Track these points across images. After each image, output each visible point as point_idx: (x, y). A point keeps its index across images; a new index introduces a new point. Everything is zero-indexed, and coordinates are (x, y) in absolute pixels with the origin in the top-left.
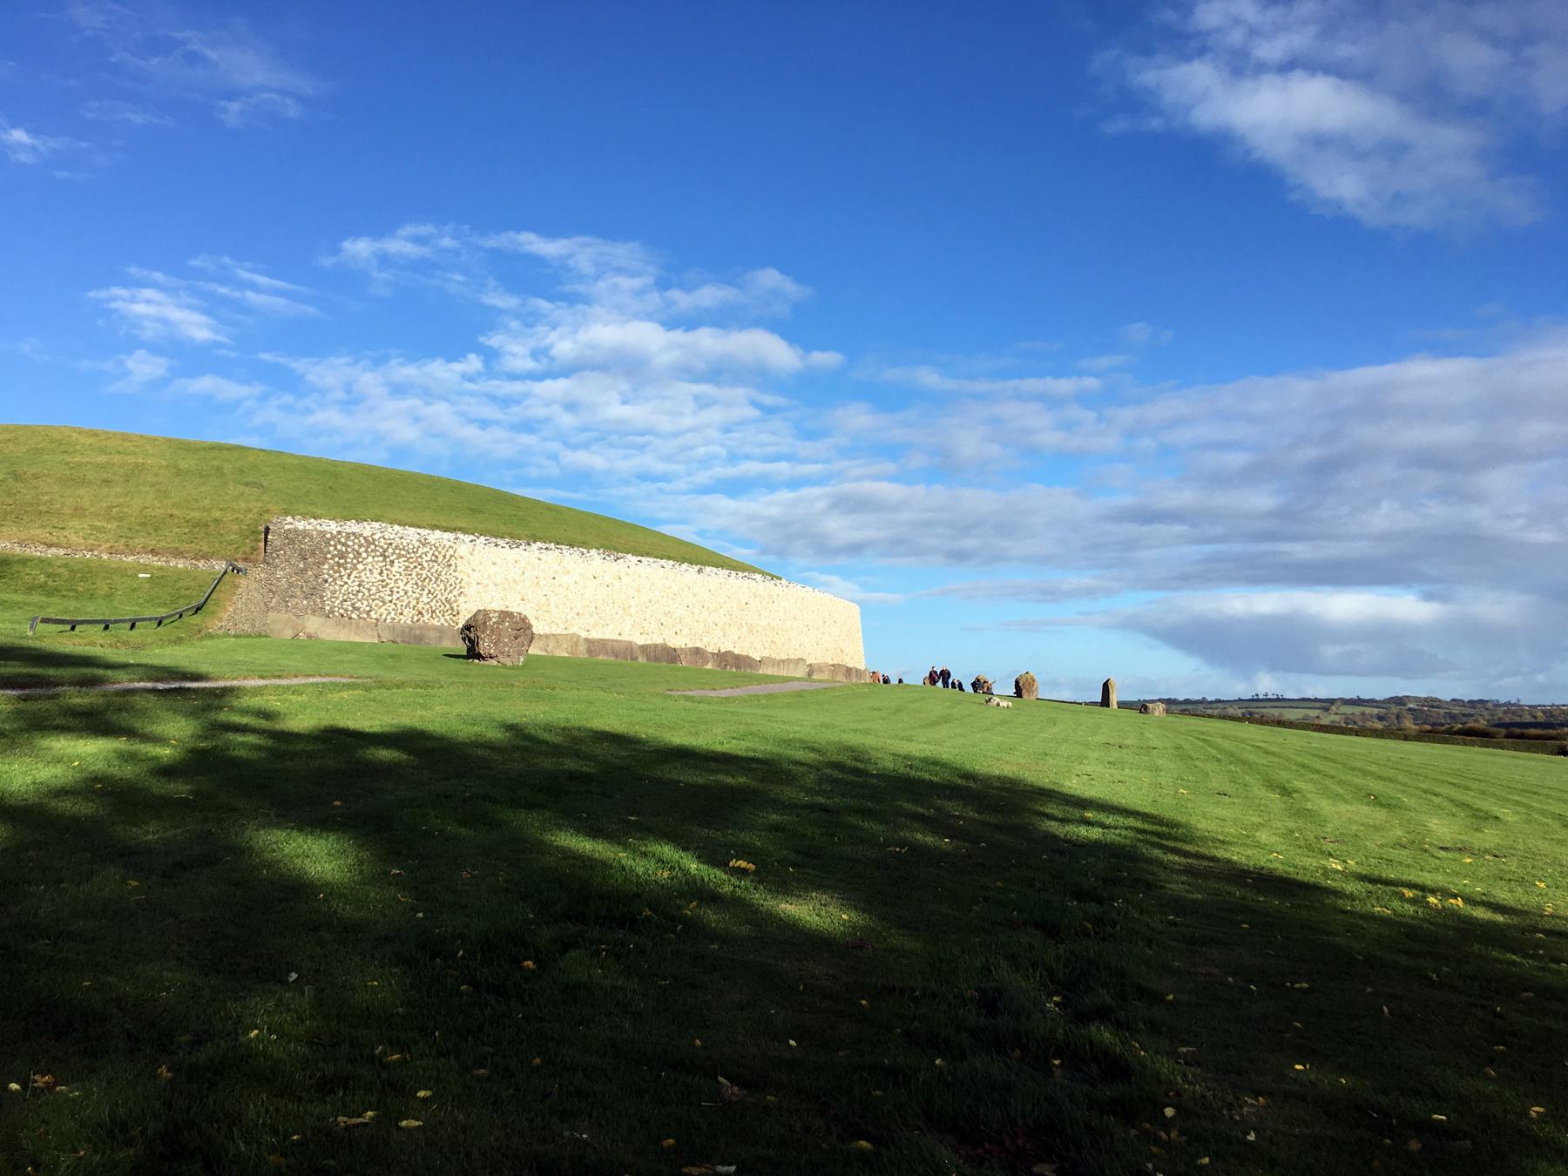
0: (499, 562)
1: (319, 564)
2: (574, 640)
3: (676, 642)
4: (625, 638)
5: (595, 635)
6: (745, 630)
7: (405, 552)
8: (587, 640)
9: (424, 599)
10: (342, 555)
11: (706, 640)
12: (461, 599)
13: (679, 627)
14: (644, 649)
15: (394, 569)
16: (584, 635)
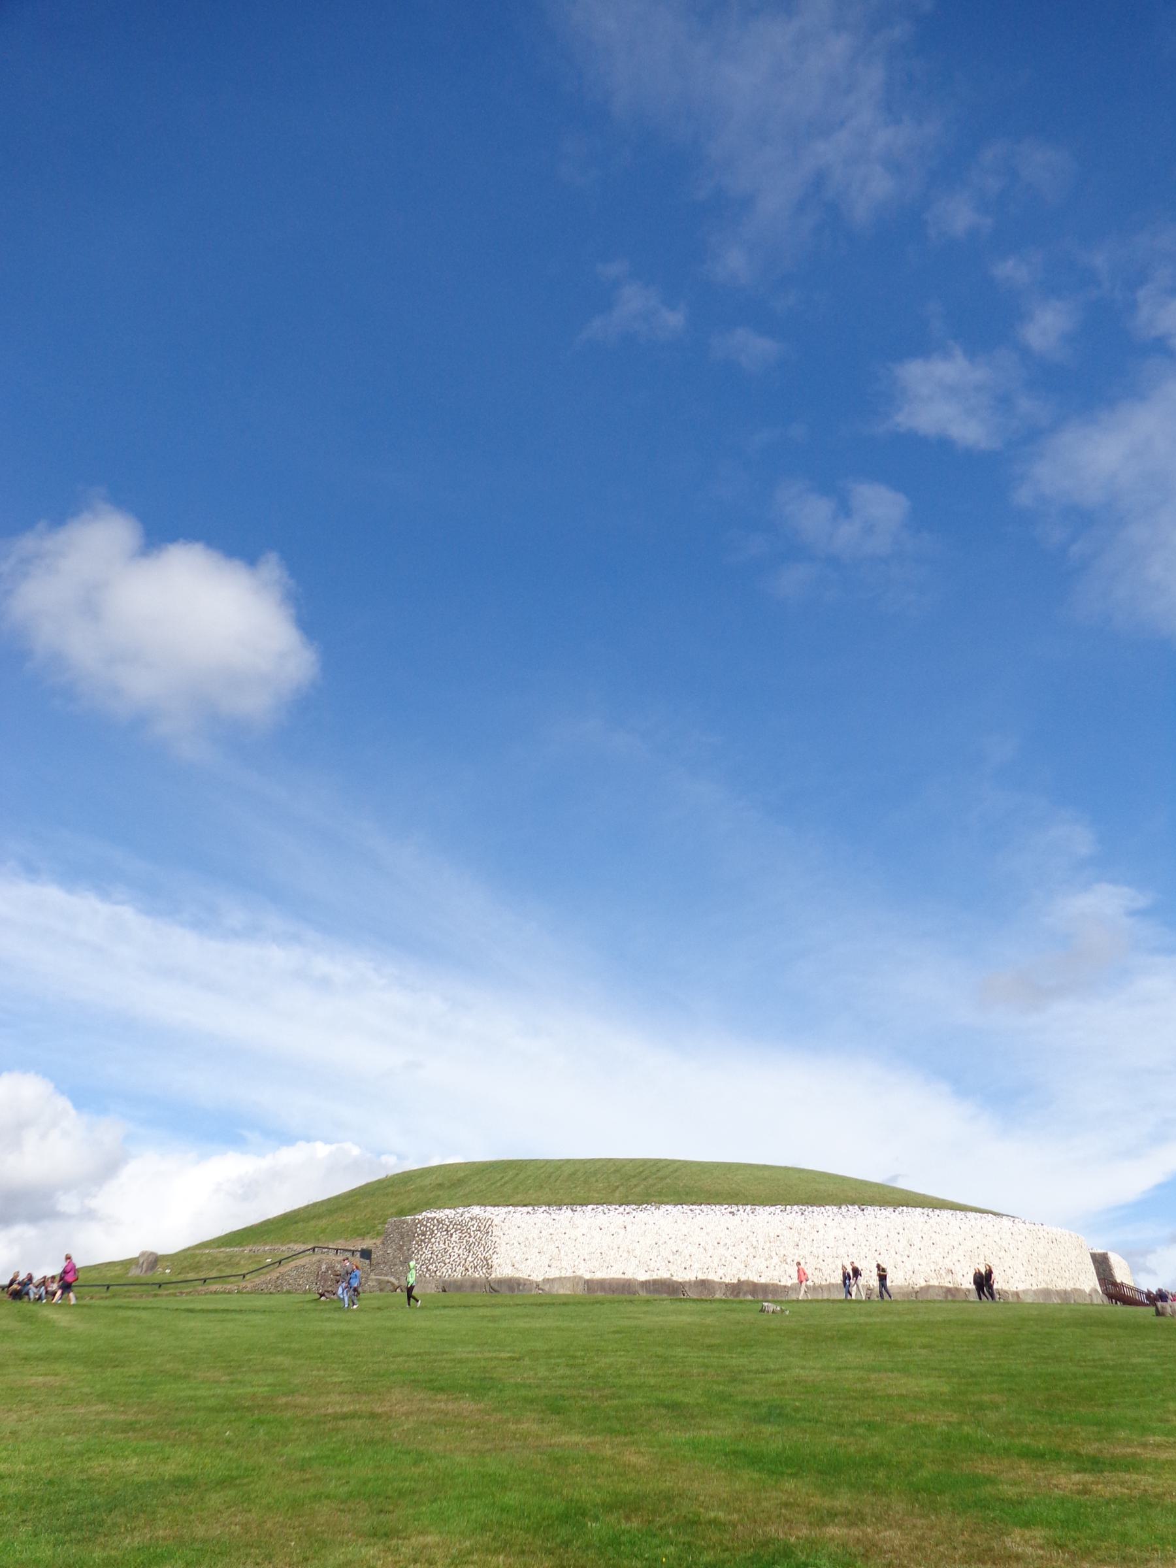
0: (523, 1225)
1: (411, 1241)
2: (576, 1280)
3: (680, 1276)
4: (629, 1276)
5: (599, 1275)
6: (776, 1260)
7: (461, 1227)
8: (587, 1282)
9: (470, 1259)
10: (424, 1234)
11: (721, 1273)
12: (495, 1256)
13: (689, 1263)
14: (645, 1285)
15: (453, 1239)
16: (587, 1276)
